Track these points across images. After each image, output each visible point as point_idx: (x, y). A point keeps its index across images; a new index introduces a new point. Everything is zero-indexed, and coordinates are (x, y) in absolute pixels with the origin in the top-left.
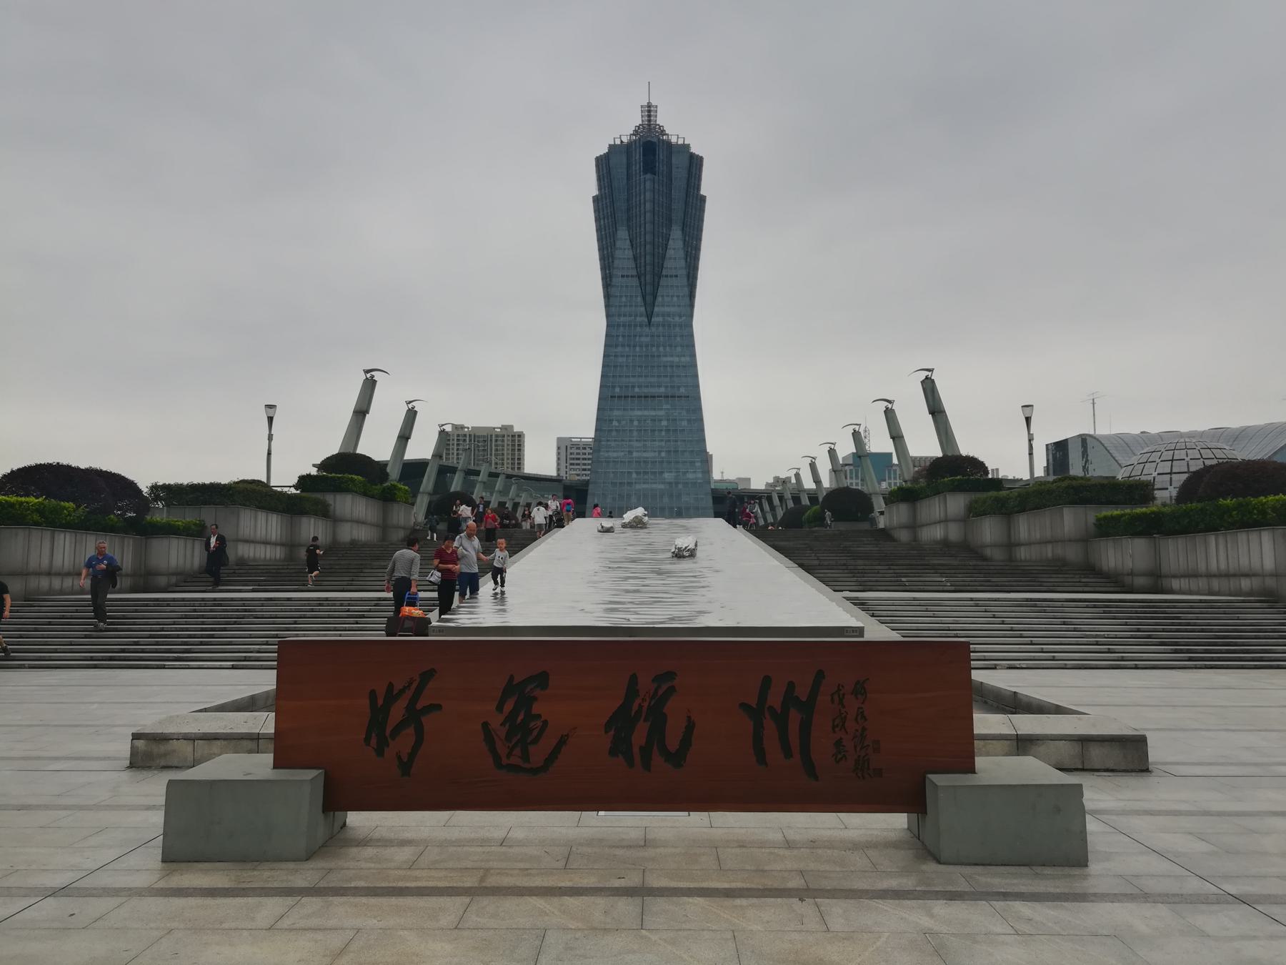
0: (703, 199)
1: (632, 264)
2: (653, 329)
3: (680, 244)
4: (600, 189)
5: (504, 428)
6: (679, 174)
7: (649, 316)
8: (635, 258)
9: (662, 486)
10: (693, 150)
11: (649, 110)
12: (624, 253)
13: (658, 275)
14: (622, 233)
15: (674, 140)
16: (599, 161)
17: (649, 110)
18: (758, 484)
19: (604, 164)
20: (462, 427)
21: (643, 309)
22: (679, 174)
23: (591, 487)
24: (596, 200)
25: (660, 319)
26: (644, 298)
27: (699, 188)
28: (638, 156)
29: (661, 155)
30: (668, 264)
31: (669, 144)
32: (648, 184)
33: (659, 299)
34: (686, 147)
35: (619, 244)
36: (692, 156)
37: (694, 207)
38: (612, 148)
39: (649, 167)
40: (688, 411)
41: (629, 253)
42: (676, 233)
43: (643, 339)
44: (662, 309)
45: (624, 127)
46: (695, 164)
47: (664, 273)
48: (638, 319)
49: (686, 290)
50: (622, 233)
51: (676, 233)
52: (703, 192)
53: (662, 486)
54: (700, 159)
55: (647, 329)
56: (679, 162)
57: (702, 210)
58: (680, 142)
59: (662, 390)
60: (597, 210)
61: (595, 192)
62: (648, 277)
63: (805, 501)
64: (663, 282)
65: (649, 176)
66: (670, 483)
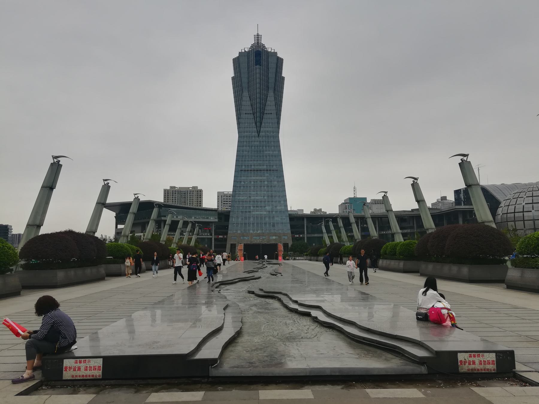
0: (283, 78)
1: (250, 108)
2: (261, 138)
3: (273, 98)
4: (235, 73)
5: (193, 187)
6: (272, 71)
7: (259, 132)
8: (252, 106)
9: (265, 213)
10: (278, 55)
11: (258, 37)
12: (246, 102)
13: (262, 113)
14: (246, 94)
15: (270, 50)
17: (258, 37)
18: (332, 208)
19: (236, 62)
20: (175, 187)
21: (255, 129)
22: (272, 66)
23: (231, 213)
24: (233, 79)
25: (264, 134)
26: (256, 124)
27: (281, 73)
28: (252, 58)
29: (264, 57)
30: (267, 108)
31: (268, 52)
32: (258, 71)
33: (263, 124)
34: (276, 53)
35: (244, 98)
36: (278, 58)
37: (279, 82)
38: (240, 53)
39: (258, 62)
40: (277, 177)
41: (249, 103)
42: (271, 94)
43: (255, 143)
44: (265, 129)
45: (247, 44)
46: (279, 62)
47: (265, 112)
48: (253, 134)
49: (276, 120)
50: (246, 94)
51: (271, 94)
52: (283, 75)
53: (265, 213)
55: (258, 138)
56: (272, 61)
58: (273, 51)
59: (265, 167)
61: (233, 75)
63: (429, 224)
64: (265, 116)
65: (258, 66)
66: (269, 211)
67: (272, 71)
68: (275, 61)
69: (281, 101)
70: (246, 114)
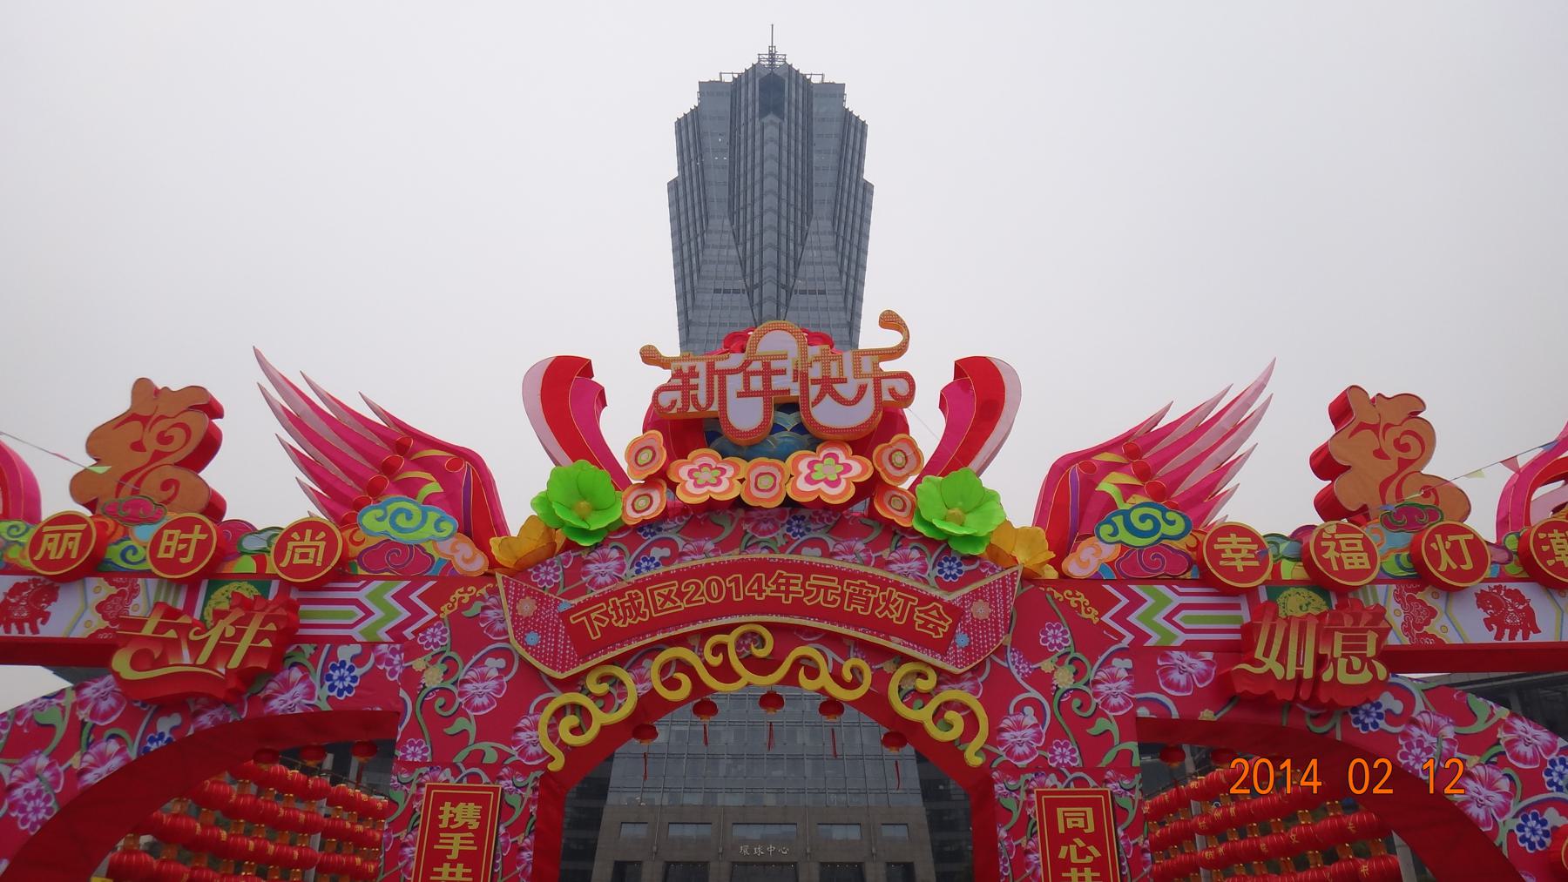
0: (868, 189)
1: (733, 270)
4: (681, 167)
14: (720, 221)
15: (816, 80)
16: (682, 126)
24: (673, 186)
27: (860, 169)
28: (750, 94)
29: (793, 94)
32: (771, 132)
36: (848, 115)
46: (852, 132)
51: (821, 223)
52: (867, 176)
54: (863, 126)
57: (866, 205)
60: (675, 203)
61: (673, 173)
62: (769, 289)
65: (771, 117)
67: (824, 160)
68: (835, 127)
69: (860, 266)
70: (717, 291)
